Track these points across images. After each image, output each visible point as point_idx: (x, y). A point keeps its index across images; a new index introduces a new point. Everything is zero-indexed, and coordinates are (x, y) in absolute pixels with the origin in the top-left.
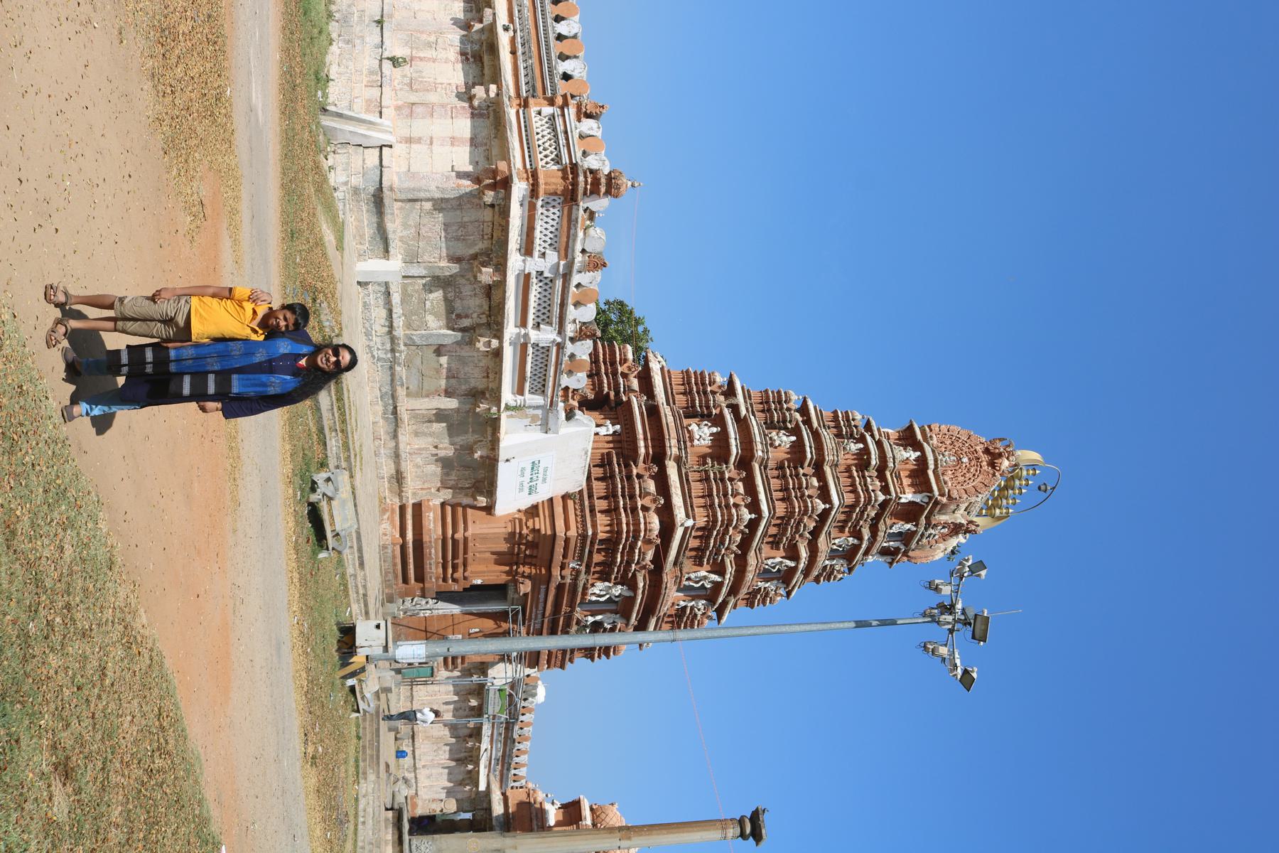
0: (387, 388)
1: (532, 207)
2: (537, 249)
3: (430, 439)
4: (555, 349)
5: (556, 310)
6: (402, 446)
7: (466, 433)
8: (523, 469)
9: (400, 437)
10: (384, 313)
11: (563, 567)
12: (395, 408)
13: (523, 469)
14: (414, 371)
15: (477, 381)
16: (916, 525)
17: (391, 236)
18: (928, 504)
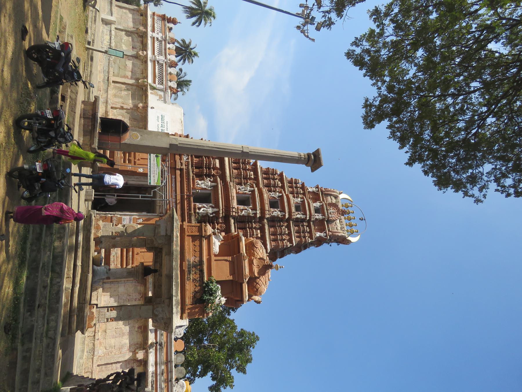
0: (106, 68)
1: (153, 19)
2: (156, 32)
3: (121, 100)
4: (164, 65)
5: (163, 51)
6: (109, 96)
7: (135, 99)
8: (158, 117)
9: (109, 92)
10: (109, 37)
11: (181, 159)
12: (108, 78)
13: (158, 117)
14: (116, 65)
15: (138, 75)
16: (321, 202)
17: (113, 12)
18: (318, 191)
